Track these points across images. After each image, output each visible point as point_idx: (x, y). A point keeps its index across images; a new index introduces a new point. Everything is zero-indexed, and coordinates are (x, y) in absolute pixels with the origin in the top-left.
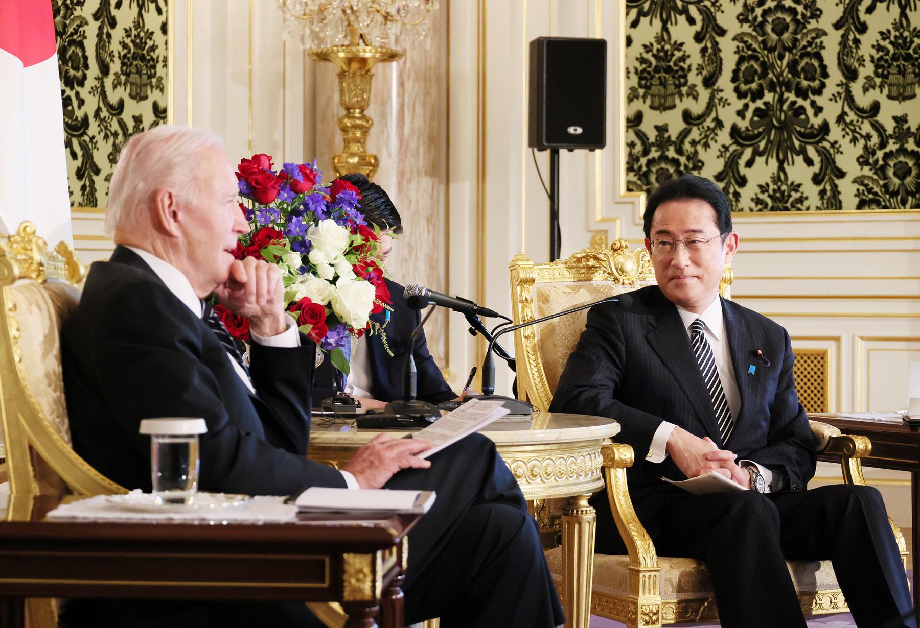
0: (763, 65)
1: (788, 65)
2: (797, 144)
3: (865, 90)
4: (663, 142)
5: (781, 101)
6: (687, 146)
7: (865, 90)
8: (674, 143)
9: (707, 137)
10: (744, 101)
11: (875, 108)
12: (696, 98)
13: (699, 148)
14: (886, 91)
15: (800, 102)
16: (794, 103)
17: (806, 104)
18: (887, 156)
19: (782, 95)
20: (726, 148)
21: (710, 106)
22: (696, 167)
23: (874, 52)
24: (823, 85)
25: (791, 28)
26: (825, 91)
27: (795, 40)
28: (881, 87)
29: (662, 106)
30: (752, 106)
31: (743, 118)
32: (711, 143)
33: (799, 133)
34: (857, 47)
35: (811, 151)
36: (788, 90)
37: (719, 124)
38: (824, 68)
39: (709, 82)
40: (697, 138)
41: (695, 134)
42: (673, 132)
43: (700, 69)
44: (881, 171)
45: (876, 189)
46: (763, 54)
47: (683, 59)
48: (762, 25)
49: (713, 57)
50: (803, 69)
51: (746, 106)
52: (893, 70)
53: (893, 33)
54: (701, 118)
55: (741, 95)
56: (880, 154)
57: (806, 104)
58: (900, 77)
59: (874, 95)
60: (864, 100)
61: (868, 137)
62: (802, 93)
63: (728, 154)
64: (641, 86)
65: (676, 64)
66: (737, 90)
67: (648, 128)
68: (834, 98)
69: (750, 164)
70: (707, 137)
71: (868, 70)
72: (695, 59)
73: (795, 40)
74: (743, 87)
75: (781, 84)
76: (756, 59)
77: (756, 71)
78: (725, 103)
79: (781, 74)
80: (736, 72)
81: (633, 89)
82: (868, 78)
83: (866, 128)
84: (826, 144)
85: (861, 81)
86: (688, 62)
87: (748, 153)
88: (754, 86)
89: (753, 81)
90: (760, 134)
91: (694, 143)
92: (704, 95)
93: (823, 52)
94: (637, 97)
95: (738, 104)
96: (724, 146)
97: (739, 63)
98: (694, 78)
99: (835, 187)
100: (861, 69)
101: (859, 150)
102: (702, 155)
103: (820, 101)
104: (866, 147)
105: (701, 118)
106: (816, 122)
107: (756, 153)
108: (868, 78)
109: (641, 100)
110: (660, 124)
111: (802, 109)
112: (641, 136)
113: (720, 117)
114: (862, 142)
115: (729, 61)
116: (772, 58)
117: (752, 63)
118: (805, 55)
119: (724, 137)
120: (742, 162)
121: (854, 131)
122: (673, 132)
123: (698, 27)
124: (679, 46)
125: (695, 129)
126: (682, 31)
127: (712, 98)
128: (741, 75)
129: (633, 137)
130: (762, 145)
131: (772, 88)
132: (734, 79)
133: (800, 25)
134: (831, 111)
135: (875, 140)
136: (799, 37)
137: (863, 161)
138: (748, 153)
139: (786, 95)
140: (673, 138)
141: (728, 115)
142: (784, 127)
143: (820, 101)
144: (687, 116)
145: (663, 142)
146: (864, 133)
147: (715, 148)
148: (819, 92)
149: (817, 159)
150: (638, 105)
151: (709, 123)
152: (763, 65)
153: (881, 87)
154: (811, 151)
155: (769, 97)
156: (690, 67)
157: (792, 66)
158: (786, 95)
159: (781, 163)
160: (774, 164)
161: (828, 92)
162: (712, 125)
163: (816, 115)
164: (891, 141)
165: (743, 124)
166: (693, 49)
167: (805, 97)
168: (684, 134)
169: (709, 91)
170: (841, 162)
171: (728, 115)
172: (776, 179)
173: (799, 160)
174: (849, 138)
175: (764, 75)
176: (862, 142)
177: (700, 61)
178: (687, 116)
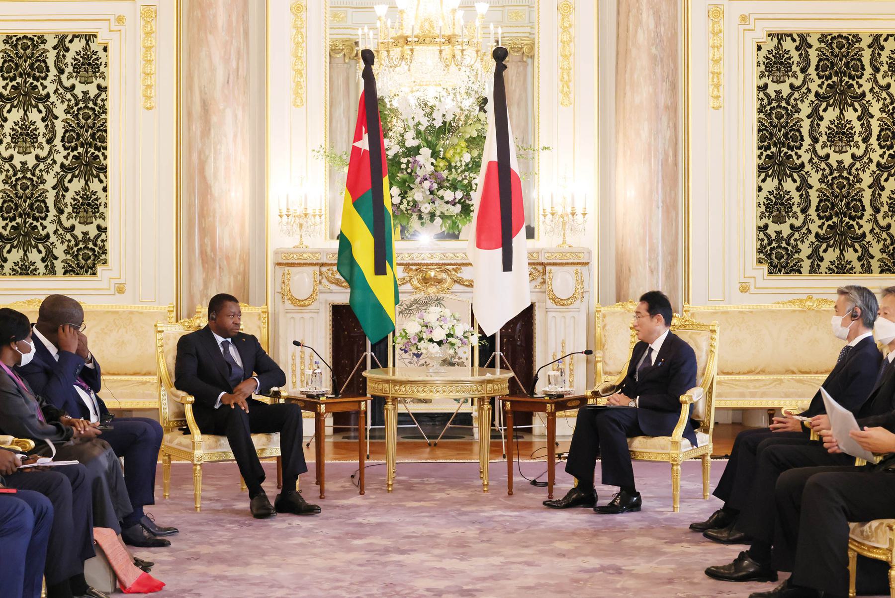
9: (48, 168)
11: (73, 87)
12: (42, 149)
17: (38, 84)
21: (50, 153)
25: (31, 48)
27: (94, 124)
31: (67, 160)
32: (50, 171)
34: (64, 59)
37: (55, 162)
43: (44, 135)
45: (73, 125)
48: (77, 115)
63: (59, 176)
65: (31, 132)
66: (63, 146)
70: (48, 168)
73: (94, 124)
74: (67, 145)
76: (13, 62)
77: (74, 137)
80: (63, 137)
89: (72, 142)
90: (76, 167)
91: (41, 171)
92: (47, 148)
95: (65, 153)
96: (57, 172)
97: (65, 133)
102: (45, 176)
115: (60, 132)
119: (57, 168)
120: (66, 180)
125: (42, 164)
126: (35, 116)
128: (66, 139)
130: (77, 173)
131: (82, 145)
132: (62, 141)
134: (51, 88)
136: (96, 122)
141: (59, 158)
142: (87, 164)
147: (52, 173)
160: (83, 182)
161: (49, 79)
164: (81, 103)
166: (41, 126)
169: (49, 146)
177: (45, 131)
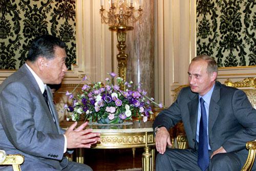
0: (227, 24)
3: (251, 30)
5: (231, 34)
7: (251, 30)
15: (235, 34)
17: (237, 34)
24: (241, 29)
38: (241, 24)
48: (226, 13)
51: (223, 36)
57: (237, 34)
60: (250, 33)
62: (236, 31)
68: (243, 33)
71: (251, 24)
73: (234, 16)
84: (242, 45)
85: (250, 27)
88: (225, 30)
99: (244, 57)
103: (240, 33)
106: (239, 39)
108: (252, 26)
111: (236, 36)
119: (218, 45)
130: (227, 46)
131: (229, 31)
134: (243, 36)
143: (240, 33)
148: (240, 31)
152: (227, 24)
155: (228, 33)
157: (233, 23)
165: (222, 41)
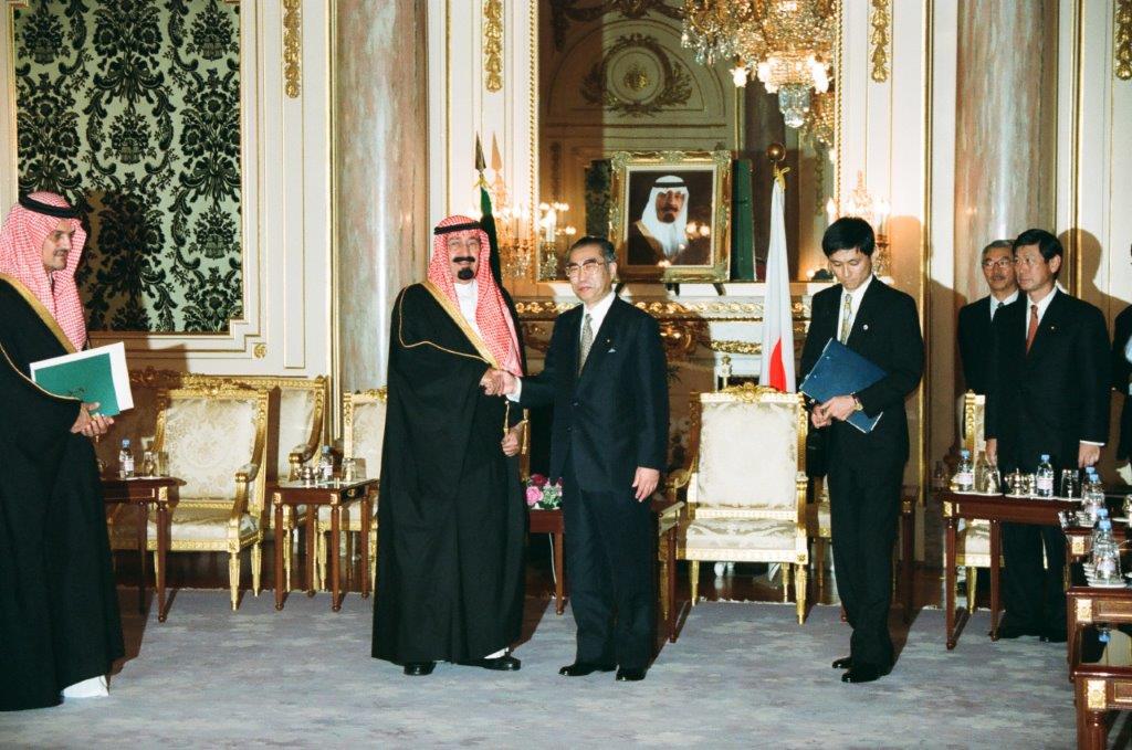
0: (203, 132)
1: (133, 32)
2: (141, 88)
4: (45, 86)
5: (216, 157)
6: (148, 188)
7: (188, 52)
8: (139, 186)
9: (163, 181)
10: (189, 157)
11: (195, 64)
12: (155, 157)
13: (157, 189)
14: (202, 53)
15: (143, 58)
16: (138, 59)
18: (204, 97)
19: (129, 53)
20: (177, 189)
22: (155, 202)
23: (193, 27)
24: (158, 47)
26: (160, 51)
27: (225, 116)
28: (199, 51)
29: (44, 61)
30: (195, 160)
33: (143, 80)
35: (152, 94)
36: (221, 150)
38: (159, 34)
39: (164, 145)
40: (156, 183)
41: (68, 81)
42: (53, 79)
43: (157, 135)
44: (200, 106)
46: (115, 24)
47: (145, 127)
49: (80, 27)
50: (231, 136)
52: (207, 40)
53: (206, 15)
54: (73, 69)
55: (186, 153)
56: (199, 95)
57: (147, 60)
58: (211, 45)
59: (193, 56)
60: (187, 59)
61: (190, 83)
62: (144, 52)
64: (28, 47)
65: (140, 131)
66: (184, 149)
67: (34, 75)
69: (194, 200)
70: (163, 181)
71: (189, 39)
72: (154, 128)
73: (225, 116)
74: (189, 148)
75: (128, 45)
78: (90, 58)
79: (129, 38)
81: (22, 49)
82: (190, 45)
83: (189, 77)
84: (162, 89)
85: (185, 46)
86: (149, 129)
87: (107, 94)
89: (195, 143)
91: (153, 186)
93: (158, 24)
94: (26, 55)
97: (185, 130)
98: (66, 42)
99: (81, 18)
100: (185, 39)
101: (184, 92)
102: (159, 193)
103: (157, 57)
104: (189, 90)
105: (73, 69)
106: (155, 73)
107: (199, 192)
108: (190, 45)
109: (114, 157)
110: (43, 73)
111: (144, 64)
112: (30, 82)
113: (87, 69)
114: (186, 87)
115: (178, 128)
116: (122, 26)
117: (108, 30)
118: (145, 25)
119: (175, 181)
120: (188, 199)
121: (180, 79)
122: (53, 79)
123: (155, 105)
124: (54, 19)
125: (154, 176)
126: (144, 108)
127: (80, 55)
129: (22, 82)
131: (209, 148)
132: (182, 142)
133: (228, 106)
134: (165, 65)
135: (195, 86)
137: (187, 100)
138: (107, 94)
139: (219, 153)
140: (53, 83)
142: (217, 175)
143: (157, 57)
144: (148, 167)
145: (45, 86)
146: (187, 80)
148: (156, 51)
149: (155, 99)
150: (26, 60)
151: (78, 73)
152: (203, 132)
153: (199, 51)
154: (152, 94)
156: (150, 133)
158: (219, 153)
159: (216, 200)
160: (211, 200)
161: (162, 51)
162: (81, 74)
163: (154, 68)
166: (152, 121)
167: (146, 55)
168: (61, 81)
170: (172, 100)
171: (178, 167)
172: (213, 210)
173: (143, 99)
174: (177, 84)
175: (116, 39)
176: (186, 87)
178: (148, 167)
